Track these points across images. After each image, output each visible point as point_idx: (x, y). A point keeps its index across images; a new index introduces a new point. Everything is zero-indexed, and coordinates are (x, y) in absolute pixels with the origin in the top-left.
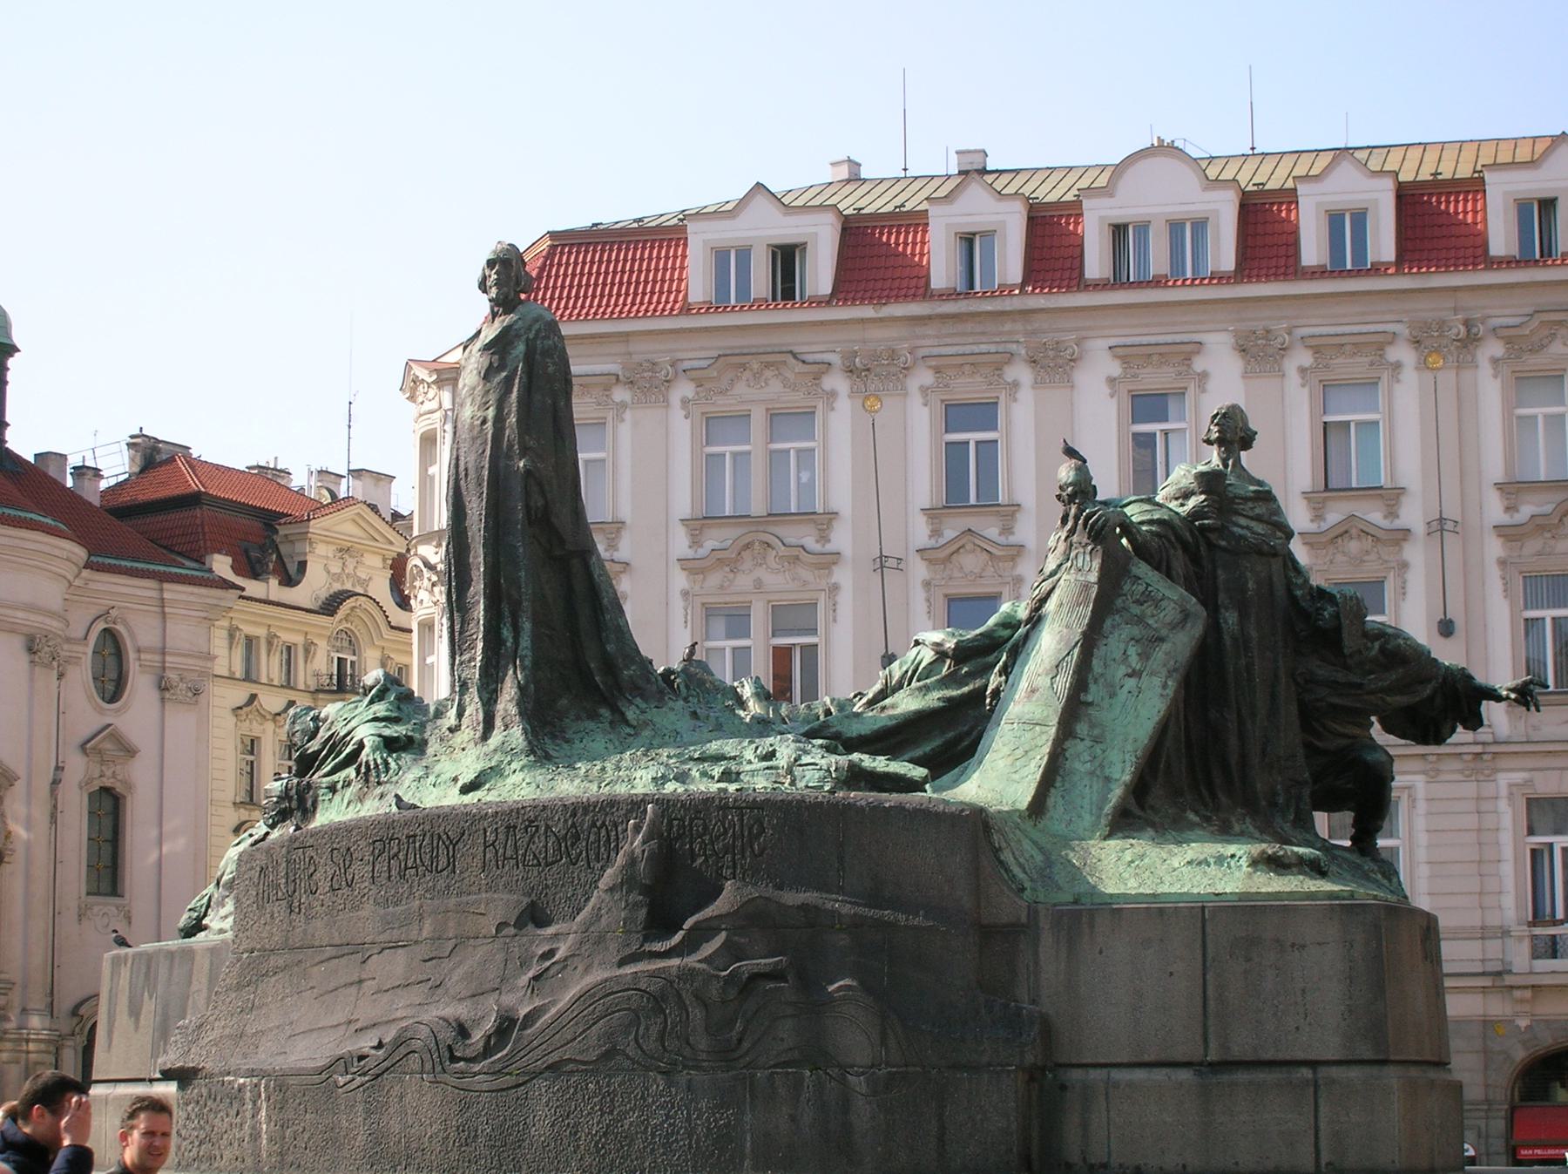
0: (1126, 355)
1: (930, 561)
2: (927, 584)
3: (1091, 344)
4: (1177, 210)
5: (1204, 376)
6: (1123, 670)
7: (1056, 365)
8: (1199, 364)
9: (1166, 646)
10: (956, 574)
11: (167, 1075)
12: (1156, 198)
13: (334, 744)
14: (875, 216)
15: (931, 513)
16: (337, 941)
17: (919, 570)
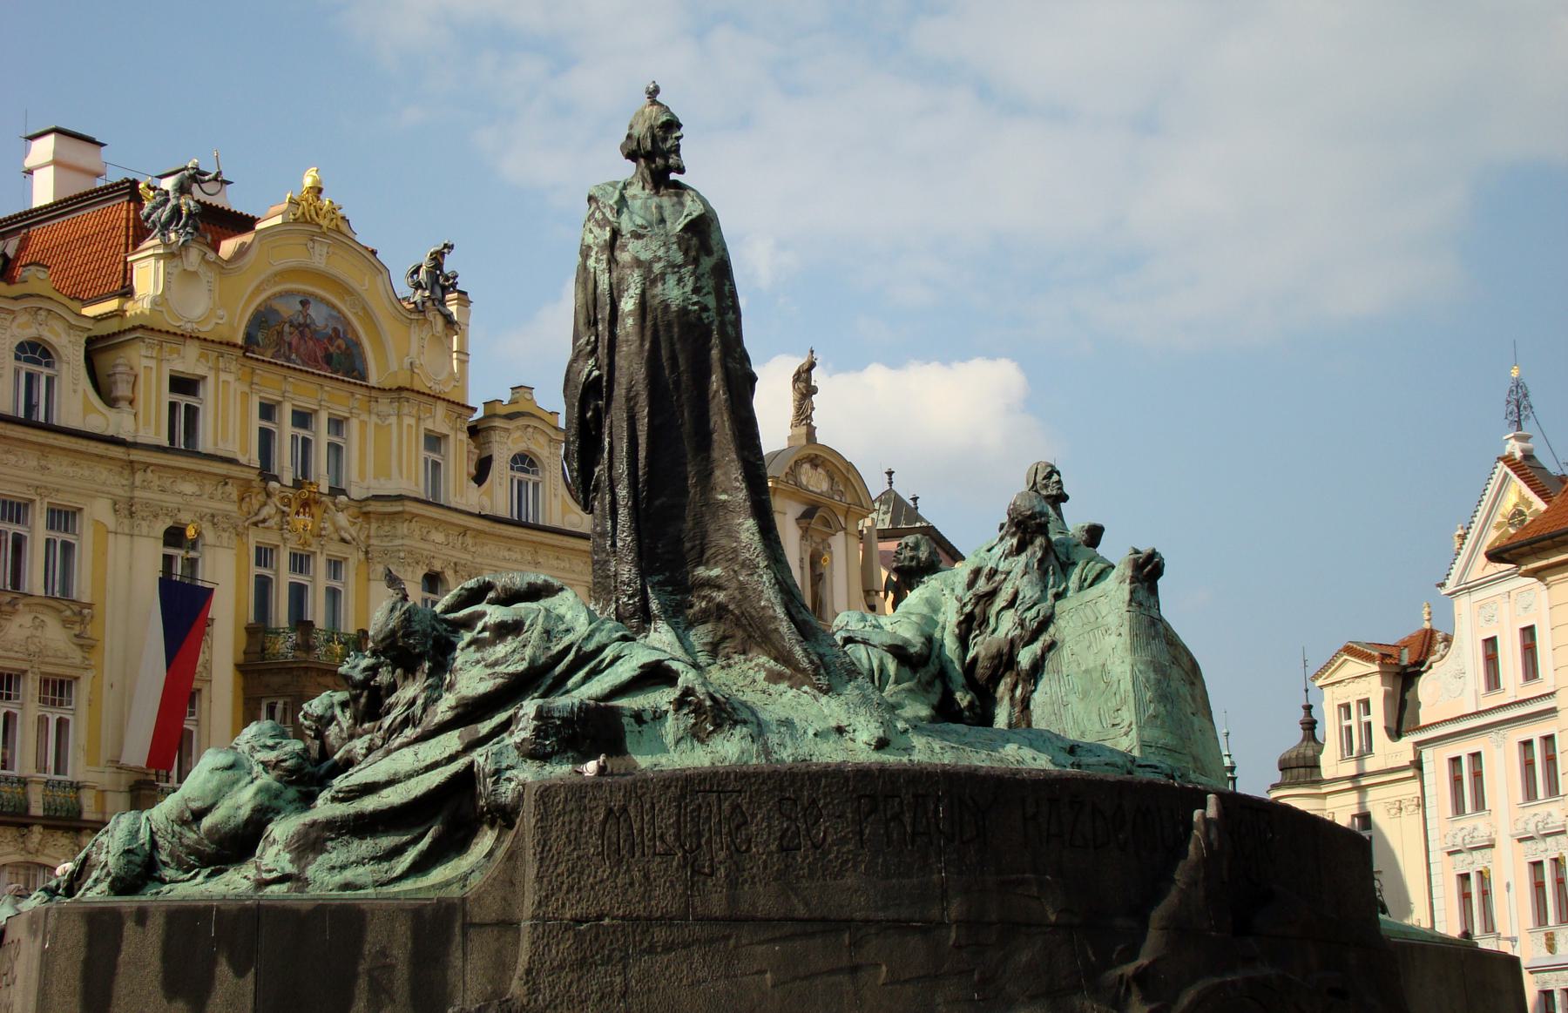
13: (587, 660)
16: (801, 911)
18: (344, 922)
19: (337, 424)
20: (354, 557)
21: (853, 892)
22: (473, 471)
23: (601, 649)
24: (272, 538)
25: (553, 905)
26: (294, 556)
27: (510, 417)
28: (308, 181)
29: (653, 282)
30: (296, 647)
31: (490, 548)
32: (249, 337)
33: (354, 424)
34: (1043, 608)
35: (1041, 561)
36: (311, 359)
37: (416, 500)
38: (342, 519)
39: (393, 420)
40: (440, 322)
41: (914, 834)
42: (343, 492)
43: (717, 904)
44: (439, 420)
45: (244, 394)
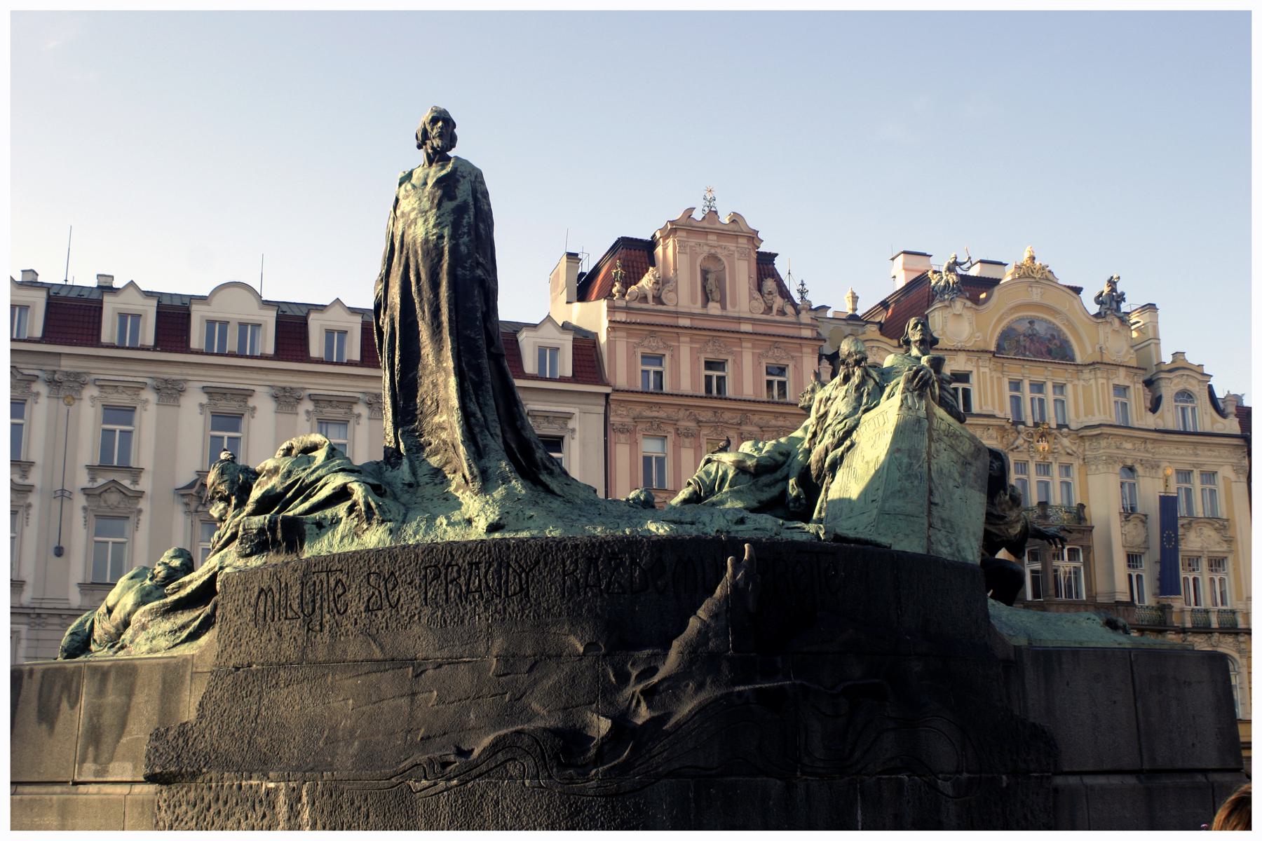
0: (210, 391)
1: (88, 495)
2: (85, 509)
3: (191, 384)
4: (245, 318)
5: (254, 409)
6: (951, 484)
7: (170, 391)
8: (252, 402)
9: (974, 469)
10: (102, 504)
11: (151, 779)
12: (236, 310)
13: (305, 490)
14: (66, 298)
15: (91, 468)
16: (378, 654)
17: (80, 501)
18: (128, 671)
19: (1060, 388)
20: (1076, 464)
21: (419, 640)
22: (1149, 405)
23: (318, 480)
24: (1025, 457)
25: (225, 655)
26: (1038, 465)
27: (1170, 371)
28: (1027, 255)
29: (409, 226)
30: (1039, 517)
31: (1165, 448)
32: (999, 347)
33: (1069, 388)
34: (850, 422)
35: (858, 388)
36: (1042, 355)
37: (1111, 426)
38: (1066, 442)
39: (1092, 382)
40: (1117, 322)
41: (468, 592)
42: (1067, 426)
43: (321, 654)
44: (1121, 378)
45: (999, 378)
